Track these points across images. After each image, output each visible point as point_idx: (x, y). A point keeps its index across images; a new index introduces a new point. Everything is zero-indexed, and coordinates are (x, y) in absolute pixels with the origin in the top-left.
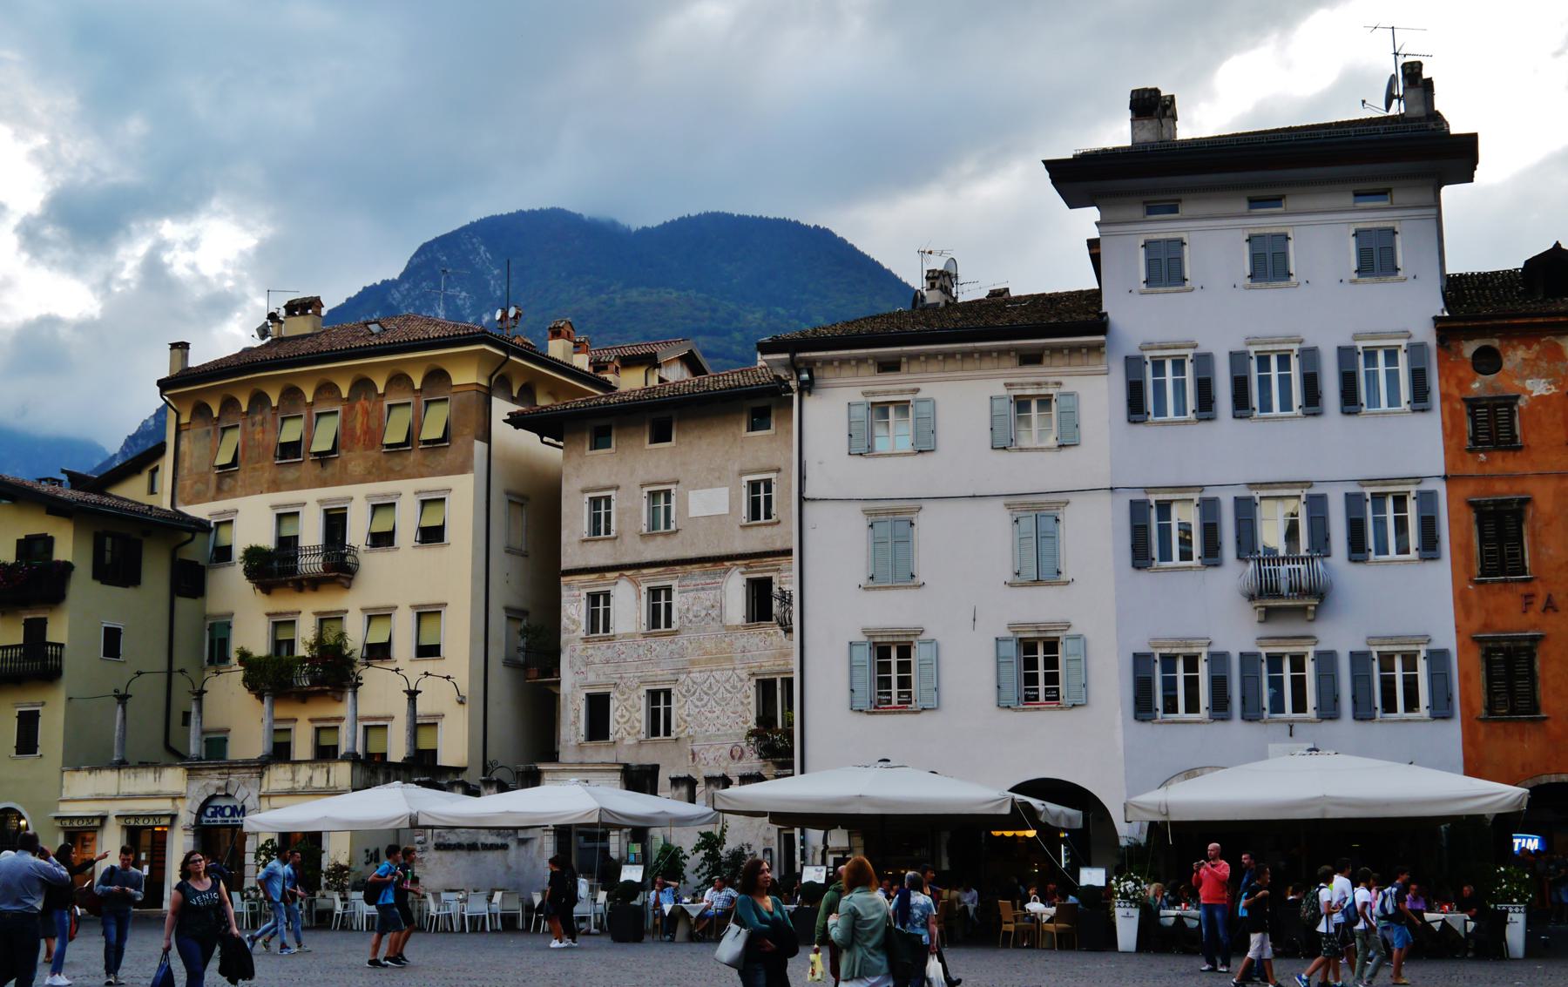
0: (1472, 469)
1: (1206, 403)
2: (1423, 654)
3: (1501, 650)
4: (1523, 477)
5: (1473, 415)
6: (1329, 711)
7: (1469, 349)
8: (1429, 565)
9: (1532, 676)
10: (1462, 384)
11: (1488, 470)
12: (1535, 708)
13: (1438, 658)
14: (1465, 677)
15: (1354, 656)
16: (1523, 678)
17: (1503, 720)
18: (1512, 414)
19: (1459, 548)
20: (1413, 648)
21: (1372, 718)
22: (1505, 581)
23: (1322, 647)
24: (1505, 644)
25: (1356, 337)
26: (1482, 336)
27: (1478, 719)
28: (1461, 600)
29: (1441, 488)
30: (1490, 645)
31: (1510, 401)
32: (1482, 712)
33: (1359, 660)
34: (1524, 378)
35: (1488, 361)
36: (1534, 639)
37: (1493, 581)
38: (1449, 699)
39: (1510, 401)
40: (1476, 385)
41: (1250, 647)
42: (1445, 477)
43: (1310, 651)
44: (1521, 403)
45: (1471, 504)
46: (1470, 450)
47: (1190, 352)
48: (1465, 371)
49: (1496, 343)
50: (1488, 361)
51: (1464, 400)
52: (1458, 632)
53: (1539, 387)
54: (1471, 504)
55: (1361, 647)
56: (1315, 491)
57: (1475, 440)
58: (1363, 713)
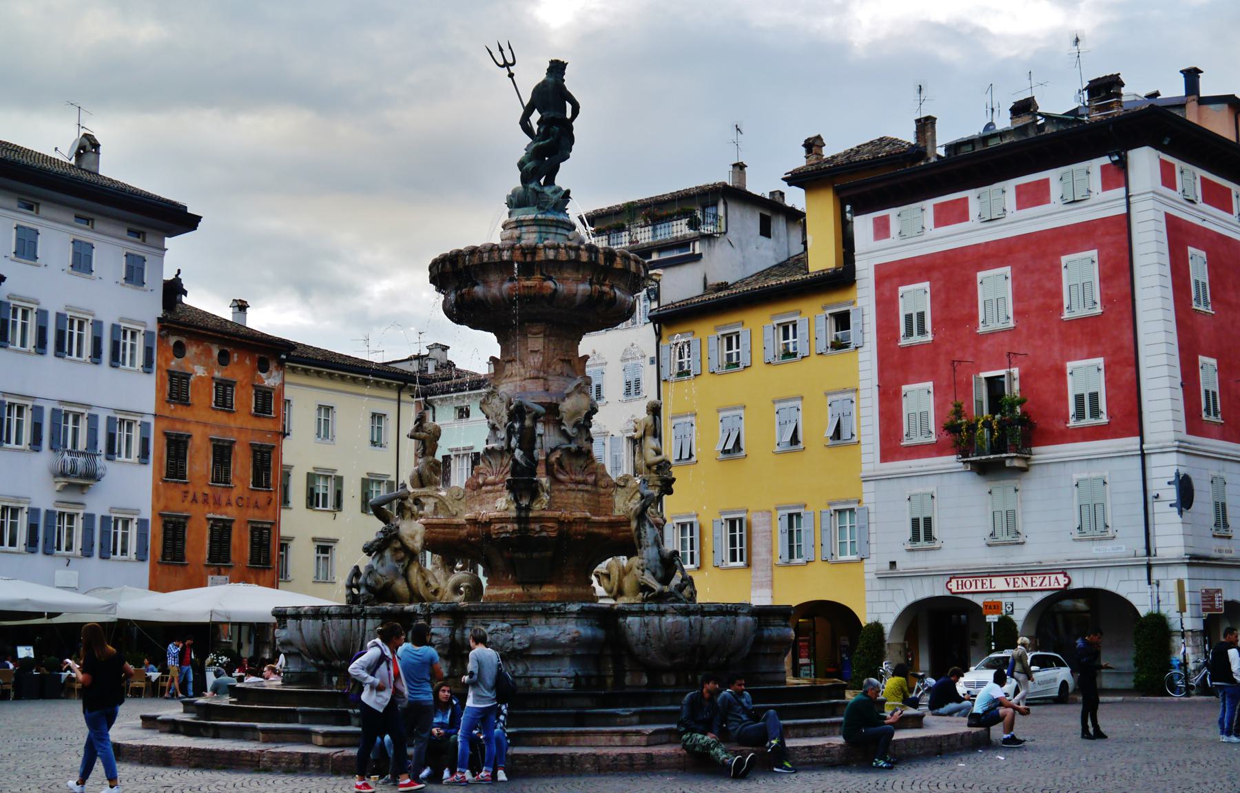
0: (167, 413)
1: (97, 354)
2: (135, 521)
3: (171, 522)
4: (189, 422)
5: (171, 381)
6: (87, 552)
7: (173, 340)
8: (143, 467)
9: (183, 539)
10: (167, 360)
11: (175, 415)
12: (183, 558)
13: (142, 523)
14: (154, 537)
15: (103, 518)
16: (179, 540)
17: (168, 564)
18: (188, 383)
19: (158, 460)
20: (131, 517)
21: (108, 558)
22: (176, 482)
23: (88, 511)
24: (173, 519)
25: (122, 320)
26: (179, 335)
27: (158, 562)
28: (156, 490)
29: (151, 420)
30: (167, 519)
31: (187, 376)
32: (159, 558)
33: (105, 520)
34: (194, 364)
35: (179, 350)
36: (187, 518)
37: (172, 482)
38: (147, 550)
39: (187, 376)
40: (173, 363)
41: (51, 507)
42: (155, 415)
43: (81, 512)
44: (192, 379)
45: (165, 434)
46: (168, 402)
47: (35, 307)
48: (170, 354)
49: (184, 340)
50: (179, 350)
51: (168, 371)
52: (153, 509)
53: (200, 371)
54: (165, 434)
55: (107, 514)
56: (93, 412)
57: (170, 396)
58: (104, 556)
